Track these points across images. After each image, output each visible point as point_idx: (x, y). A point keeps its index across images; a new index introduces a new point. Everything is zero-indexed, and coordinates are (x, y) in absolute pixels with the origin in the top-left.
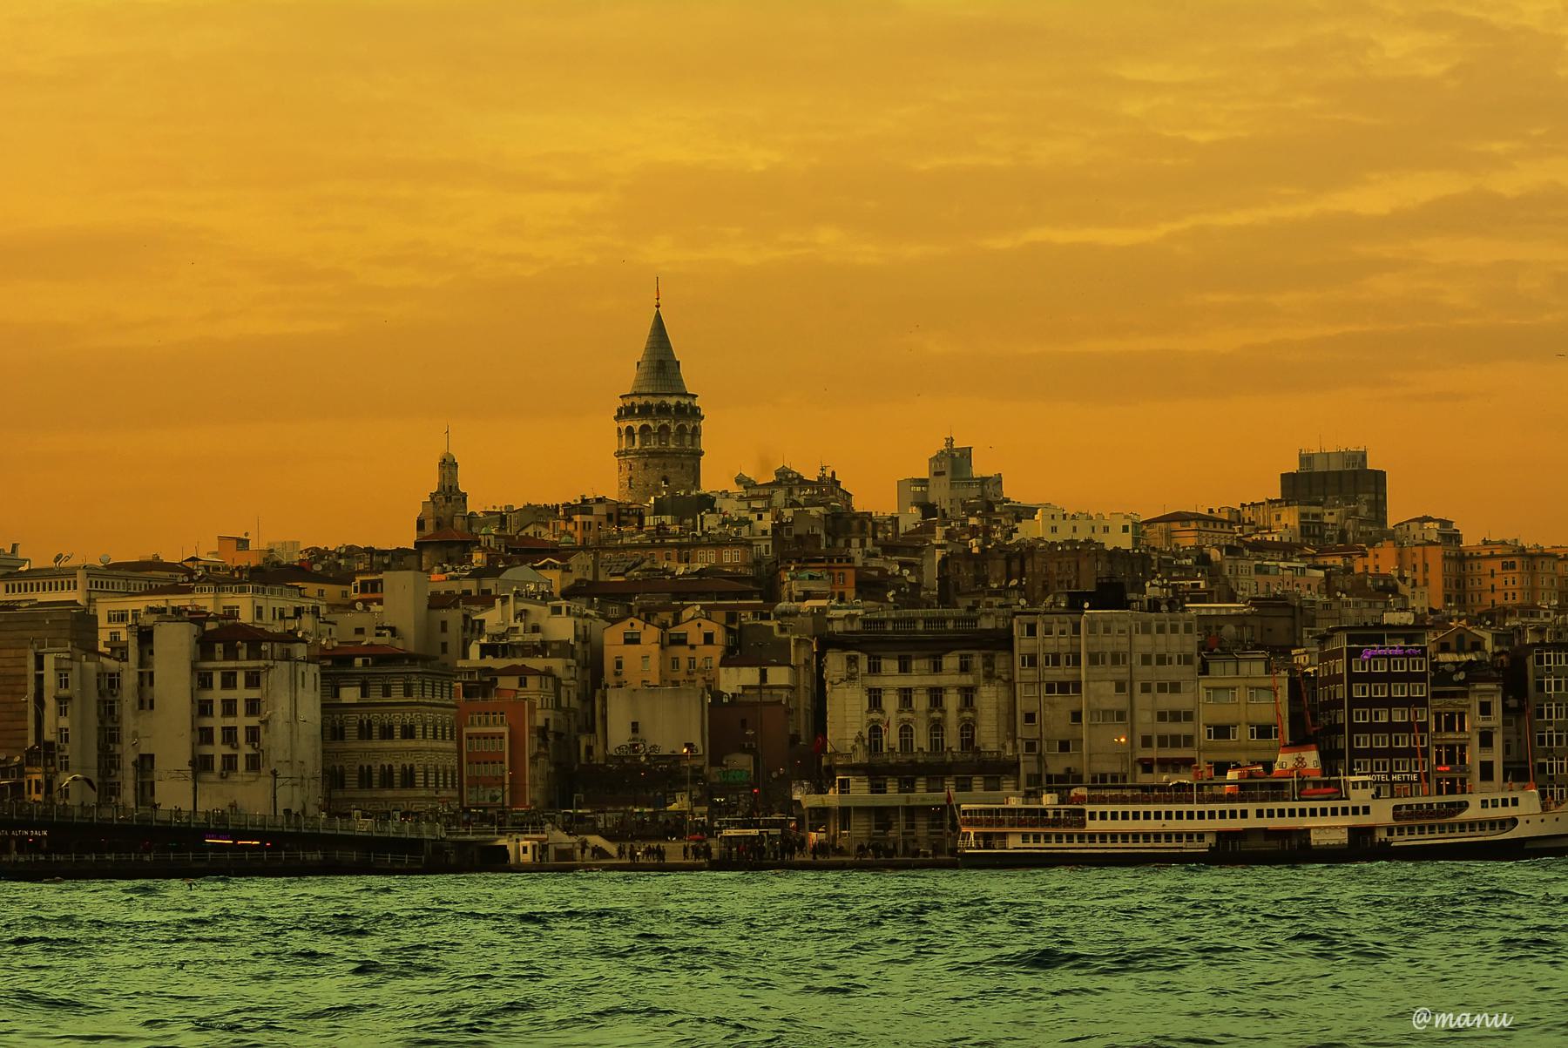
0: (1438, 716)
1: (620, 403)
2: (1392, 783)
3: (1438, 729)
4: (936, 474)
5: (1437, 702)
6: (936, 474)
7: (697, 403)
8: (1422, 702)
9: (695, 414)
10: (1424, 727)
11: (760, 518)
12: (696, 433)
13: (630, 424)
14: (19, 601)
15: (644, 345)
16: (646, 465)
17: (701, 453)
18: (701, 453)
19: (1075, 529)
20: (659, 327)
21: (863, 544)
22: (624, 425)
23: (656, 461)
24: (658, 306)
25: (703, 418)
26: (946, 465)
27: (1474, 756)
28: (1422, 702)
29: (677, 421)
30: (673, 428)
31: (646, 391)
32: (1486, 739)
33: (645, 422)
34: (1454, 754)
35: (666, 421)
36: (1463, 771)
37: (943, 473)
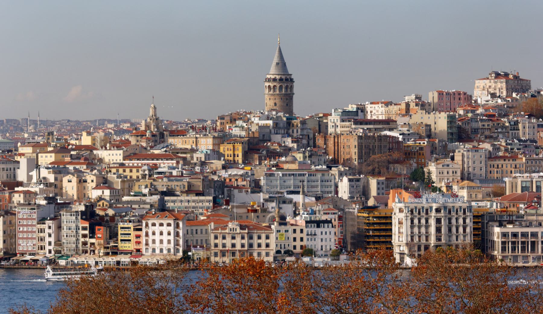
0: (38, 229)
2: (27, 246)
3: (39, 232)
5: (39, 225)
7: (292, 77)
8: (34, 226)
10: (35, 232)
12: (292, 87)
16: (270, 99)
19: (429, 118)
21: (297, 132)
23: (273, 97)
27: (47, 239)
28: (34, 226)
29: (279, 83)
30: (278, 86)
32: (50, 235)
34: (42, 239)
36: (44, 243)
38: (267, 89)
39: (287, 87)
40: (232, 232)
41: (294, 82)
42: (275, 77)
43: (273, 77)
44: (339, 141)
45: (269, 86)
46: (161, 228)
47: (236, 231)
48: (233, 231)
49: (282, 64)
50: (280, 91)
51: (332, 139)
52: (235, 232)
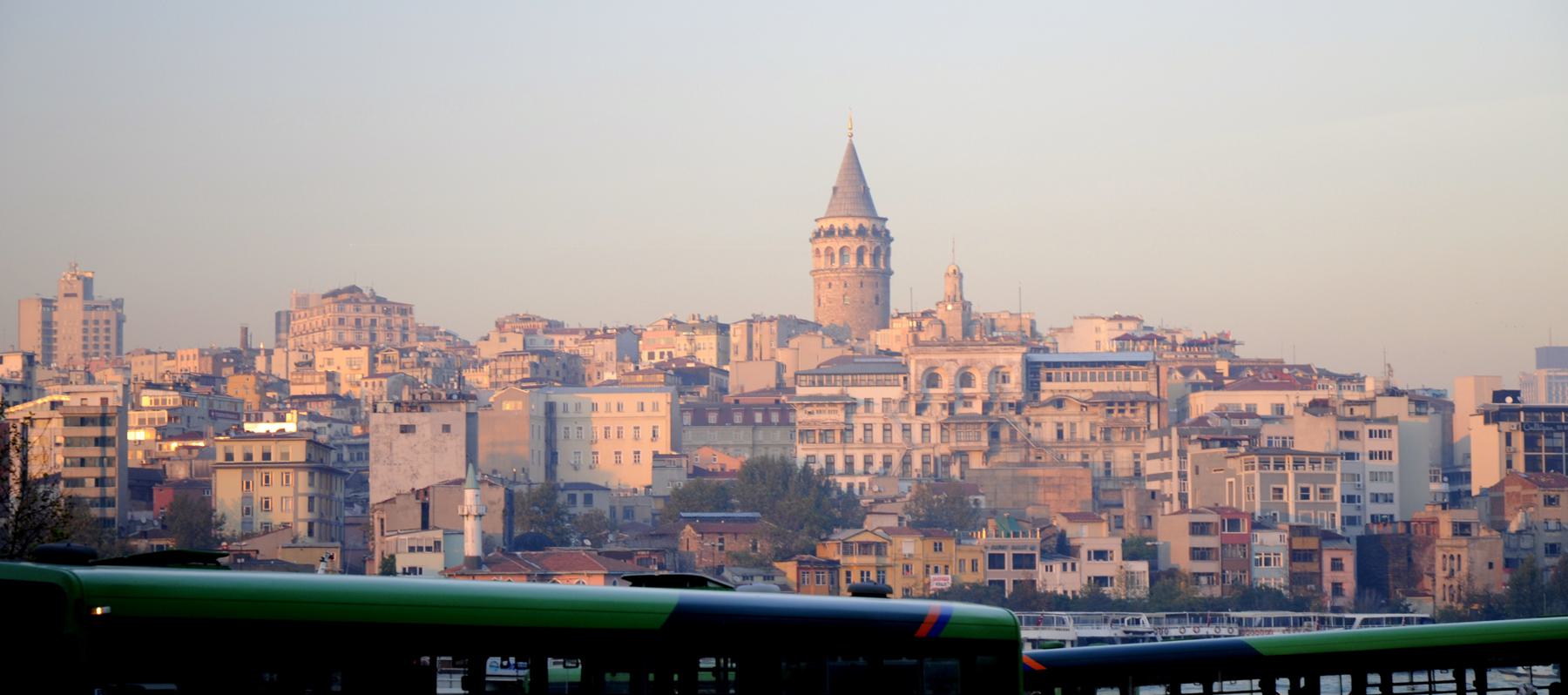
1: (816, 226)
4: (66, 295)
6: (66, 295)
9: (887, 238)
13: (847, 244)
14: (1068, 391)
15: (838, 172)
16: (862, 283)
17: (891, 273)
20: (852, 154)
22: (836, 244)
23: (871, 280)
24: (851, 136)
25: (892, 240)
26: (78, 288)
31: (856, 214)
33: (862, 244)
37: (75, 295)
38: (823, 259)
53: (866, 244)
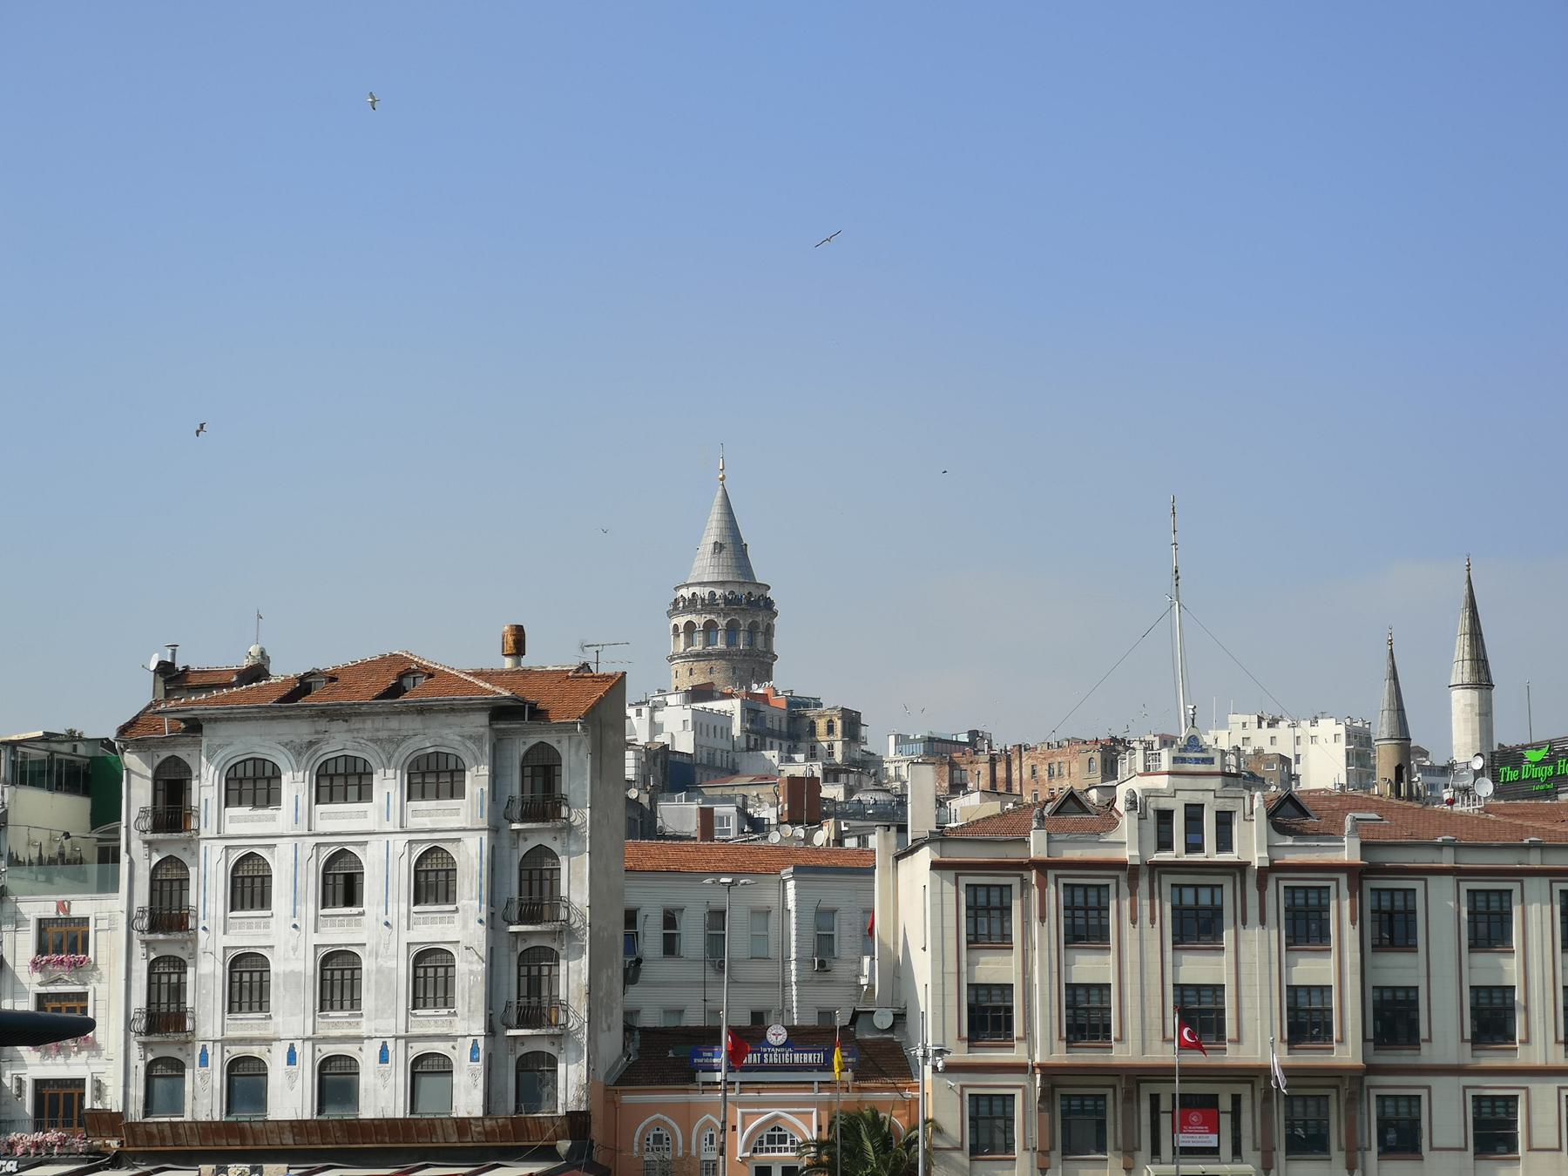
11: (639, 713)
12: (769, 631)
18: (775, 657)
30: (722, 623)
35: (713, 617)
39: (752, 630)
40: (1177, 854)
41: (776, 614)
42: (712, 594)
43: (703, 592)
44: (1015, 775)
45: (690, 627)
46: (340, 818)
47: (1224, 843)
48: (1194, 846)
49: (733, 546)
50: (728, 645)
51: (984, 769)
52: (1210, 854)
53: (693, 618)
